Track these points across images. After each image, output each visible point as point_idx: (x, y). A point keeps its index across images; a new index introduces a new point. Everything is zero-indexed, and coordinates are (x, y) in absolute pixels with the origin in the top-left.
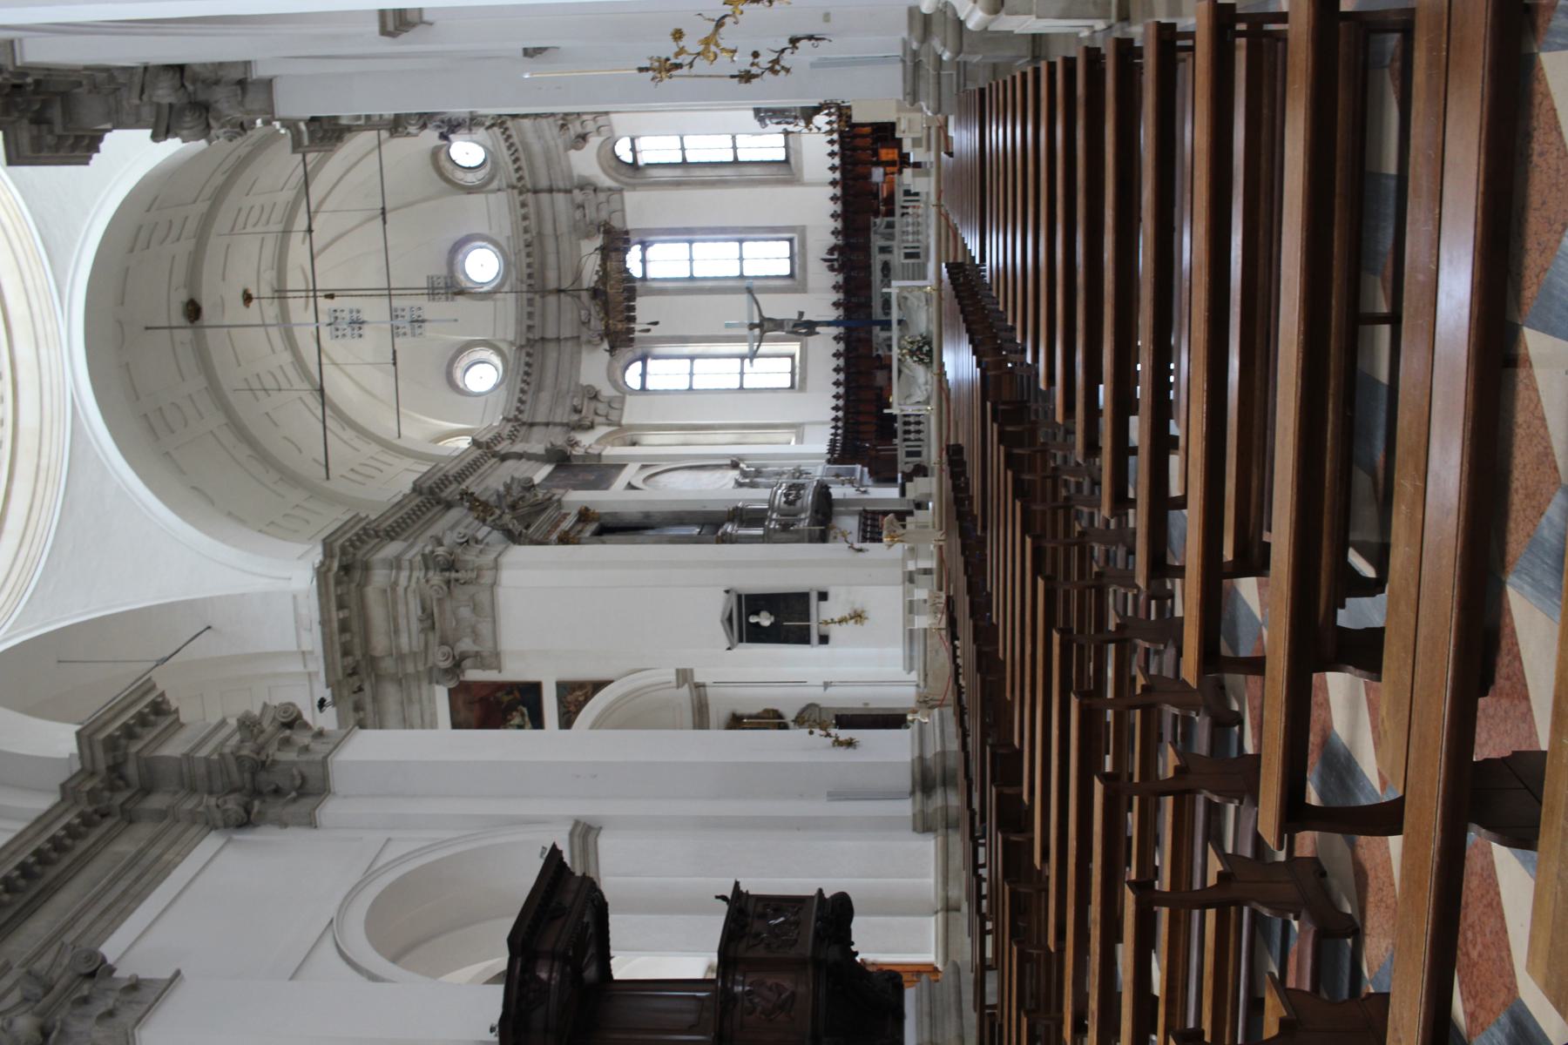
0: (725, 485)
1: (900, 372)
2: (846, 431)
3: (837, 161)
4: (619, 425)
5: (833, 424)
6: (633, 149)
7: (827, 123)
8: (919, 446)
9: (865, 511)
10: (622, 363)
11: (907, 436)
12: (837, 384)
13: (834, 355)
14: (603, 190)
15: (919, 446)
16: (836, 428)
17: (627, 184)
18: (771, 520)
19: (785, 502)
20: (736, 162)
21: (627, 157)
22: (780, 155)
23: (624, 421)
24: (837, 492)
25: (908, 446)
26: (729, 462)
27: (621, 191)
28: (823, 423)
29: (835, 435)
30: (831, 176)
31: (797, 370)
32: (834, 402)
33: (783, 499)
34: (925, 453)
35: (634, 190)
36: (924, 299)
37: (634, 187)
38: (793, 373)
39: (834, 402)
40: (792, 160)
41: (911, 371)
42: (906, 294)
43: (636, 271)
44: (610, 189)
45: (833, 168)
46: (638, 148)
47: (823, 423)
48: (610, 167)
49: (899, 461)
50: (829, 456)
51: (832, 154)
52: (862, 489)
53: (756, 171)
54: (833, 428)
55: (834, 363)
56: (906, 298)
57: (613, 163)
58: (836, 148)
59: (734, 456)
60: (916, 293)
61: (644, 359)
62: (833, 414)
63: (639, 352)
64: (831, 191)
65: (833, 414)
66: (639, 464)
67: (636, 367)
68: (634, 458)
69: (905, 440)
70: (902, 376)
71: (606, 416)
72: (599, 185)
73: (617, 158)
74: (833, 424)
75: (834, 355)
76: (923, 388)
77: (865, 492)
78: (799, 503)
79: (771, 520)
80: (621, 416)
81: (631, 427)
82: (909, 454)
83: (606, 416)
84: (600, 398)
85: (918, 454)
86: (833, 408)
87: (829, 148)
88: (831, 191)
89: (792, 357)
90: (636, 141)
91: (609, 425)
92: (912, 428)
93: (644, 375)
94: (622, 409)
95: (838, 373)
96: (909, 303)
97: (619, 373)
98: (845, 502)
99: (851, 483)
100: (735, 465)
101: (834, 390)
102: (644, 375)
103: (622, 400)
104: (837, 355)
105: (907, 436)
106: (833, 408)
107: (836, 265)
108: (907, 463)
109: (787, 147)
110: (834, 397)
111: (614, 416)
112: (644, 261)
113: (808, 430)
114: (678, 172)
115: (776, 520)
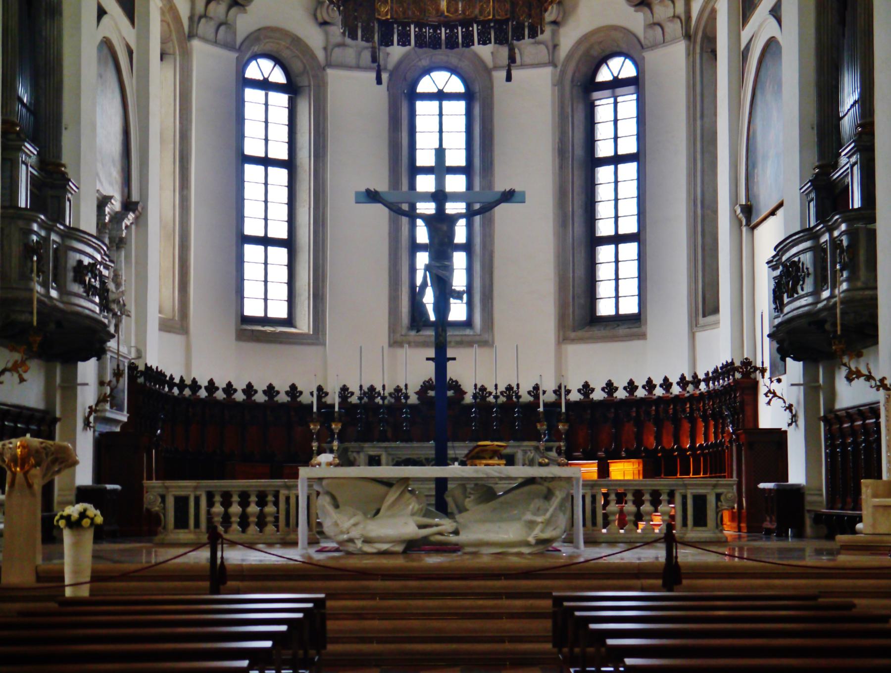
0: (100, 181)
1: (388, 483)
2: (181, 399)
3: (598, 395)
4: (191, 36)
5: (188, 382)
6: (617, 84)
7: (666, 379)
8: (197, 525)
9: (55, 420)
10: (286, 54)
11: (218, 498)
12: (249, 390)
13: (293, 387)
14: (555, 34)
15: (197, 525)
16: (182, 385)
17: (563, 73)
18: (49, 229)
19: (80, 262)
20: (594, 241)
21: (604, 75)
22: (605, 308)
23: (196, 44)
24: (87, 370)
25: (197, 500)
26: (135, 197)
27: (553, 63)
28: (188, 365)
29: (171, 383)
30: (574, 385)
31: (269, 329)
32: (221, 383)
33: (86, 261)
34: (183, 535)
35: (554, 85)
36: (546, 535)
37: (559, 83)
38: (265, 321)
39: (221, 383)
40: (596, 331)
41: (393, 505)
42: (559, 496)
43: (425, 85)
44: (555, 46)
45: (586, 389)
46: (619, 91)
47: (188, 365)
48: (591, 47)
49: (168, 483)
50: (141, 368)
51: (610, 387)
52: (92, 419)
53: (580, 272)
54: (182, 379)
55: (282, 387)
56: (548, 496)
57: (596, 52)
58: (621, 394)
59: (145, 208)
60: (562, 521)
61: (291, 88)
62: (203, 382)
63: (303, 81)
64: (549, 386)
65: (203, 382)
66: (133, 46)
67: (278, 77)
68: (144, 37)
69: (210, 496)
70: (382, 489)
71: (205, 16)
72: (563, 31)
73: (604, 60)
74: (188, 382)
75: (293, 387)
76: (355, 533)
77: (87, 424)
78: (77, 288)
79: (49, 229)
80: (205, 40)
81: (186, 54)
82: (181, 503)
83: (205, 16)
84: (234, 10)
85: (181, 522)
86: (211, 382)
87: (620, 383)
88: (549, 386)
89: (289, 321)
90: (632, 88)
91: (191, 19)
92: (235, 509)
93: (265, 85)
94: (215, 43)
95: (265, 392)
96: (538, 503)
97: (268, 47)
98: (71, 386)
99: (101, 400)
100: (129, 206)
101: (240, 385)
102: (265, 85)
103: (229, 46)
104: (293, 391)
105: (218, 498)
106: (211, 382)
107: (432, 393)
108: (163, 498)
109: (618, 319)
110: (229, 385)
111: (206, 29)
112: (441, 96)
113: (176, 339)
114: (579, 152)
115: (46, 239)
